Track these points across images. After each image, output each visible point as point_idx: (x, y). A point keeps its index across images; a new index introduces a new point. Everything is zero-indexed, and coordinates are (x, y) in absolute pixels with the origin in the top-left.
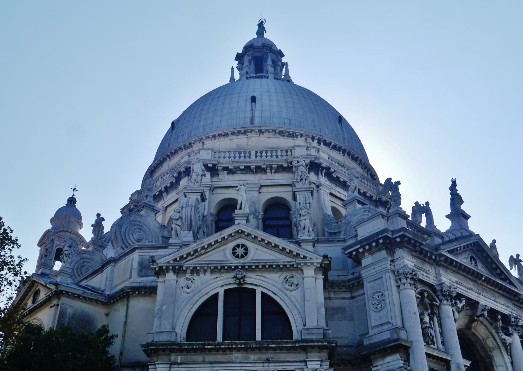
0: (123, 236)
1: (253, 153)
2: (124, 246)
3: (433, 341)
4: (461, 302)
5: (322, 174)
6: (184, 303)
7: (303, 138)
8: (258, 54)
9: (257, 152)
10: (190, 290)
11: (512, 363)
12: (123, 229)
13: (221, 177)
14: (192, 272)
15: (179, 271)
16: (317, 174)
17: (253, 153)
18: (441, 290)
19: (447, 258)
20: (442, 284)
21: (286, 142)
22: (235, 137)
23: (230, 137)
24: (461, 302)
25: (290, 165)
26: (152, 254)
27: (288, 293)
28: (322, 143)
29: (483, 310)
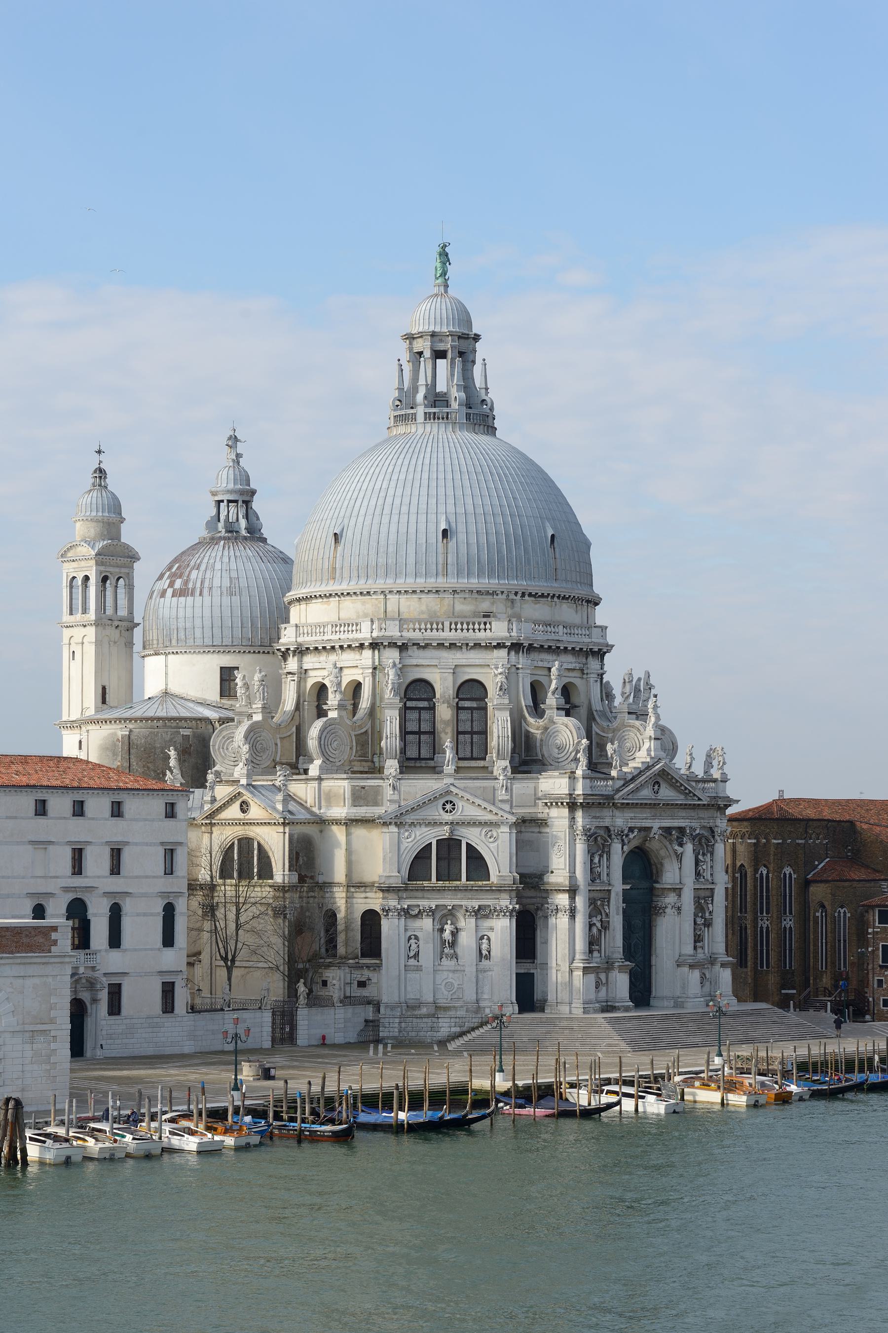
0: (323, 750)
1: (447, 624)
3: (600, 875)
4: (633, 832)
5: (523, 652)
6: (406, 852)
8: (441, 347)
9: (451, 624)
11: (680, 868)
12: (322, 742)
13: (410, 652)
15: (399, 825)
16: (517, 652)
17: (447, 624)
21: (485, 605)
22: (423, 596)
24: (633, 832)
28: (527, 597)
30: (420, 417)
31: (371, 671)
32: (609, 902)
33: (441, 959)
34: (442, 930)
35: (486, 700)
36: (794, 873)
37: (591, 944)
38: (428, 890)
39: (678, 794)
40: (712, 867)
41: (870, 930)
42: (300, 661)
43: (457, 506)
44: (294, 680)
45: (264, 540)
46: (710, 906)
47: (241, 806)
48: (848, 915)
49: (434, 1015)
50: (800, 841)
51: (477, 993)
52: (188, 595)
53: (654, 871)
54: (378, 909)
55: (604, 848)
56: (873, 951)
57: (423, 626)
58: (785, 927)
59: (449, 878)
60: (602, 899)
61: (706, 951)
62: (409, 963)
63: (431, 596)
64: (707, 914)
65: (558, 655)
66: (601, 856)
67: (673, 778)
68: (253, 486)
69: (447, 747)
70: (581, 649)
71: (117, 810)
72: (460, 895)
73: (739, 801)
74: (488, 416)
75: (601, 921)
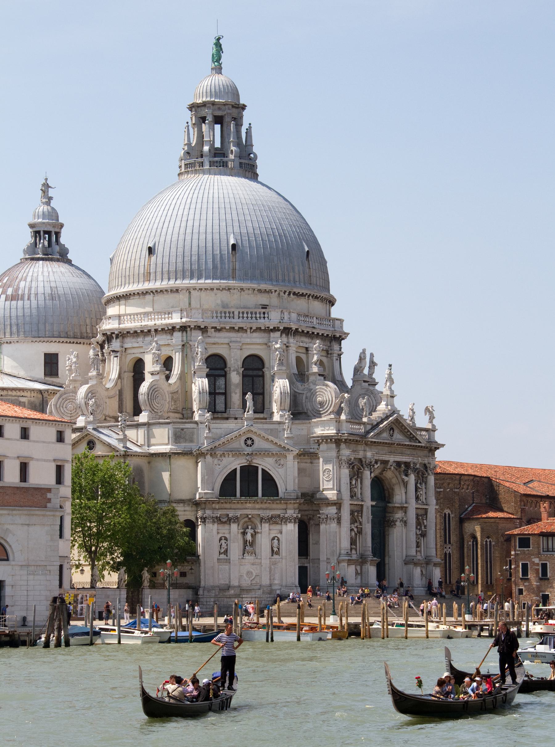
1: (236, 313)
2: (151, 410)
3: (355, 494)
5: (291, 335)
7: (277, 293)
9: (239, 313)
10: (220, 466)
11: (406, 493)
12: (150, 398)
13: (209, 334)
14: (221, 456)
16: (287, 335)
17: (236, 313)
18: (365, 462)
19: (372, 442)
20: (365, 458)
21: (263, 299)
22: (219, 291)
23: (215, 291)
25: (266, 328)
26: (181, 427)
27: (277, 469)
29: (391, 466)
30: (207, 167)
31: (180, 347)
32: (362, 513)
33: (243, 555)
34: (244, 533)
35: (263, 370)
36: (452, 513)
37: (351, 544)
38: (234, 503)
39: (405, 438)
40: (426, 493)
41: (513, 553)
42: (122, 342)
43: (241, 227)
44: (117, 357)
45: (69, 262)
46: (425, 521)
47: (88, 444)
48: (493, 543)
49: (240, 595)
50: (456, 490)
51: (270, 579)
52: (18, 300)
53: (387, 495)
54: (194, 519)
55: (358, 475)
56: (515, 567)
57: (219, 315)
58: (446, 553)
59: (249, 494)
60: (358, 511)
61: (423, 555)
62: (220, 557)
63: (224, 291)
64: (423, 528)
65: (312, 339)
66: (356, 480)
67: (403, 425)
68: (61, 221)
69: (247, 398)
70: (328, 335)
71: (25, 434)
72: (257, 506)
73: (443, 445)
74: (254, 166)
75: (357, 527)
